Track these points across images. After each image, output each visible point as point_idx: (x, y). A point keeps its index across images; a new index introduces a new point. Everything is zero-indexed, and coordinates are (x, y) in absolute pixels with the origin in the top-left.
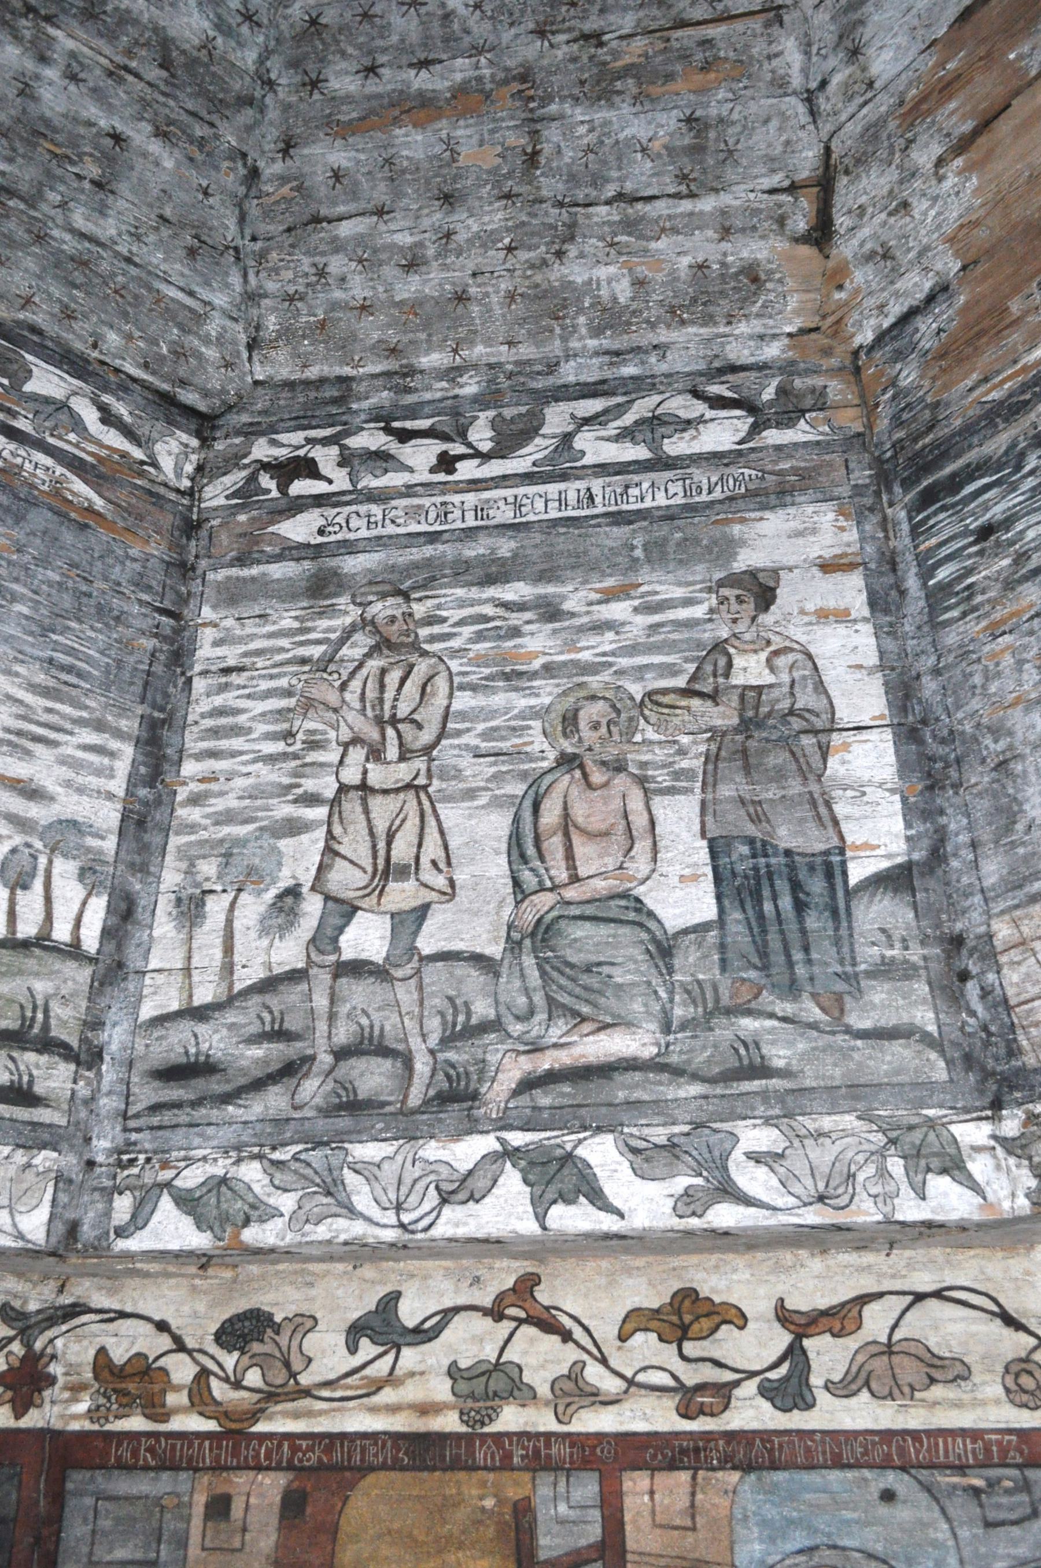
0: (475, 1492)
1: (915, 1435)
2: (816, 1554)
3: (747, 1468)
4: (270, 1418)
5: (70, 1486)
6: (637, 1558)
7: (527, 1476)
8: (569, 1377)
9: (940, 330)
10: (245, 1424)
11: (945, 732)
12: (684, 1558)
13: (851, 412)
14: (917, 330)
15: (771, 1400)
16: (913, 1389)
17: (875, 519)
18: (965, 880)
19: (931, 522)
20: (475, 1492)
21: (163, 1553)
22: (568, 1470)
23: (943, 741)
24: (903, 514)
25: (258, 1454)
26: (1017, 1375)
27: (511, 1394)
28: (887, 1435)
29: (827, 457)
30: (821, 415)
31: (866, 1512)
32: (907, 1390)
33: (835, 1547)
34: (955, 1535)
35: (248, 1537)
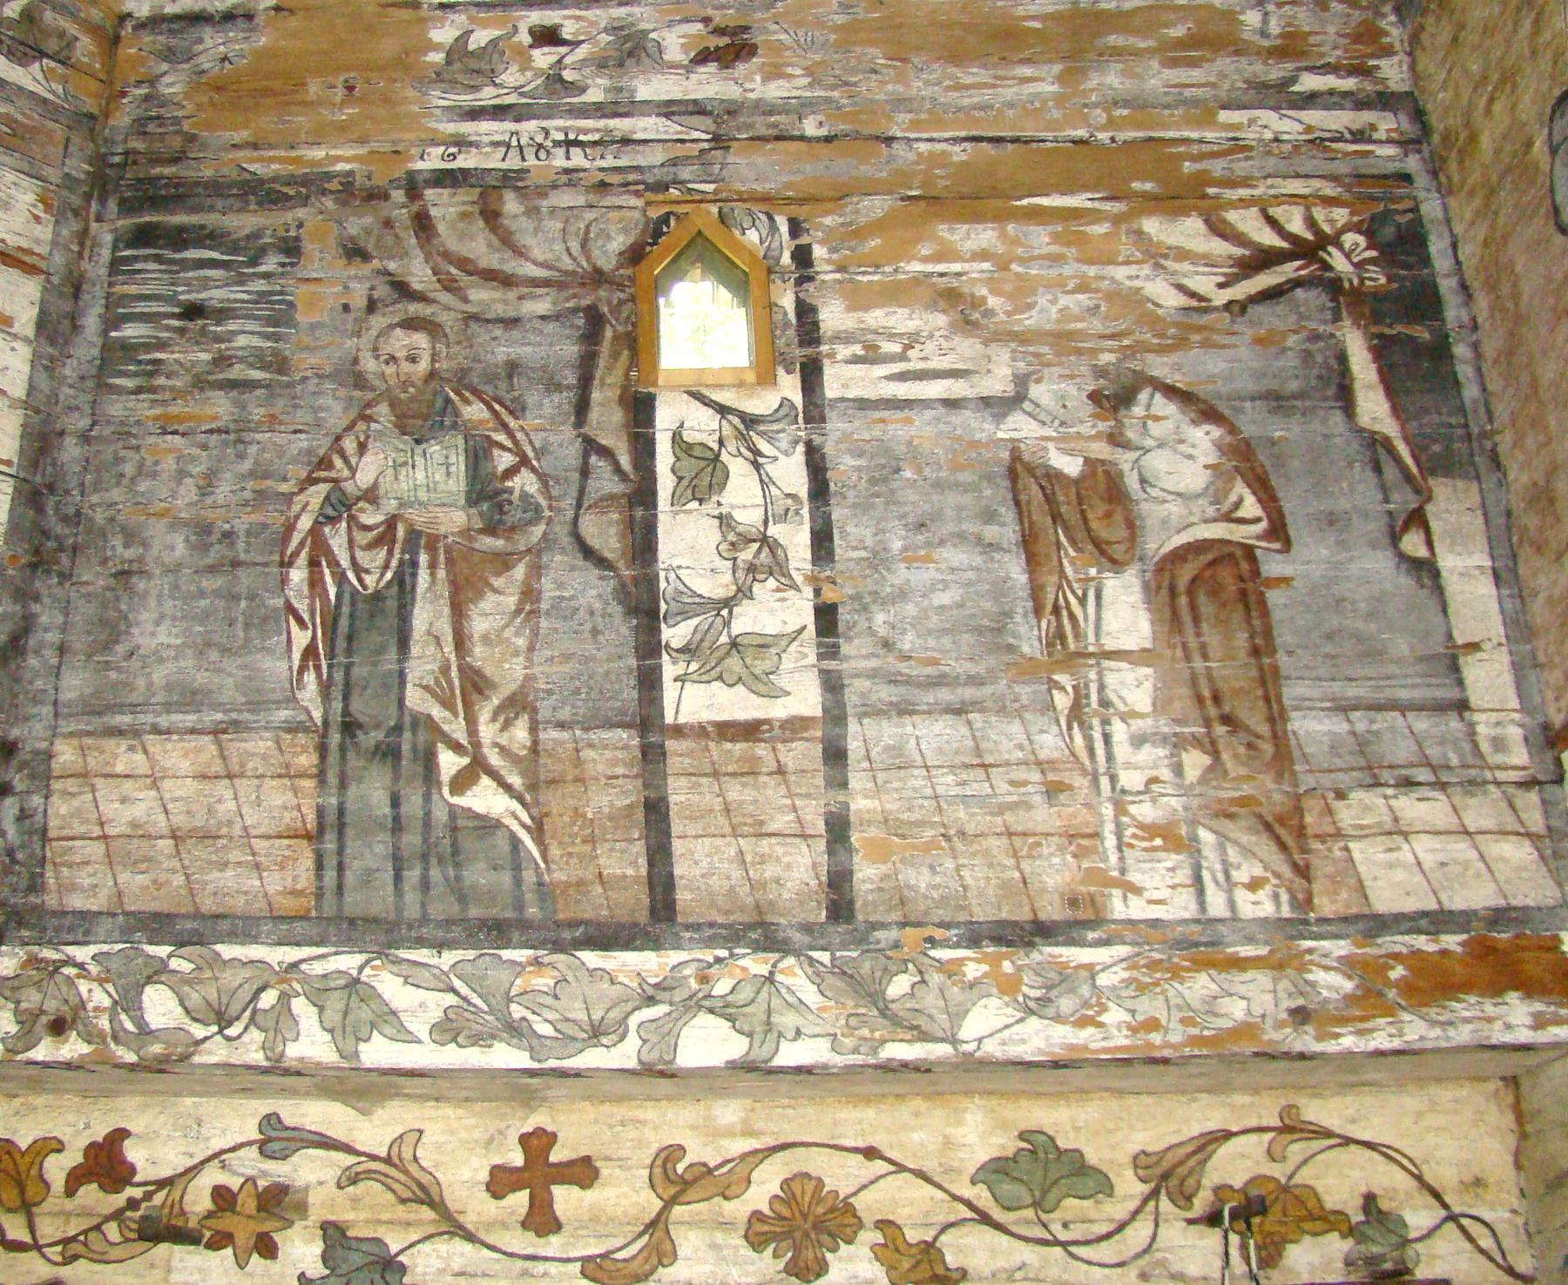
9: (225, 59)
11: (71, 511)
13: (93, 85)
14: (200, 41)
17: (76, 226)
18: (39, 684)
19: (138, 266)
23: (65, 519)
24: (109, 238)
29: (51, 125)
30: (60, 69)
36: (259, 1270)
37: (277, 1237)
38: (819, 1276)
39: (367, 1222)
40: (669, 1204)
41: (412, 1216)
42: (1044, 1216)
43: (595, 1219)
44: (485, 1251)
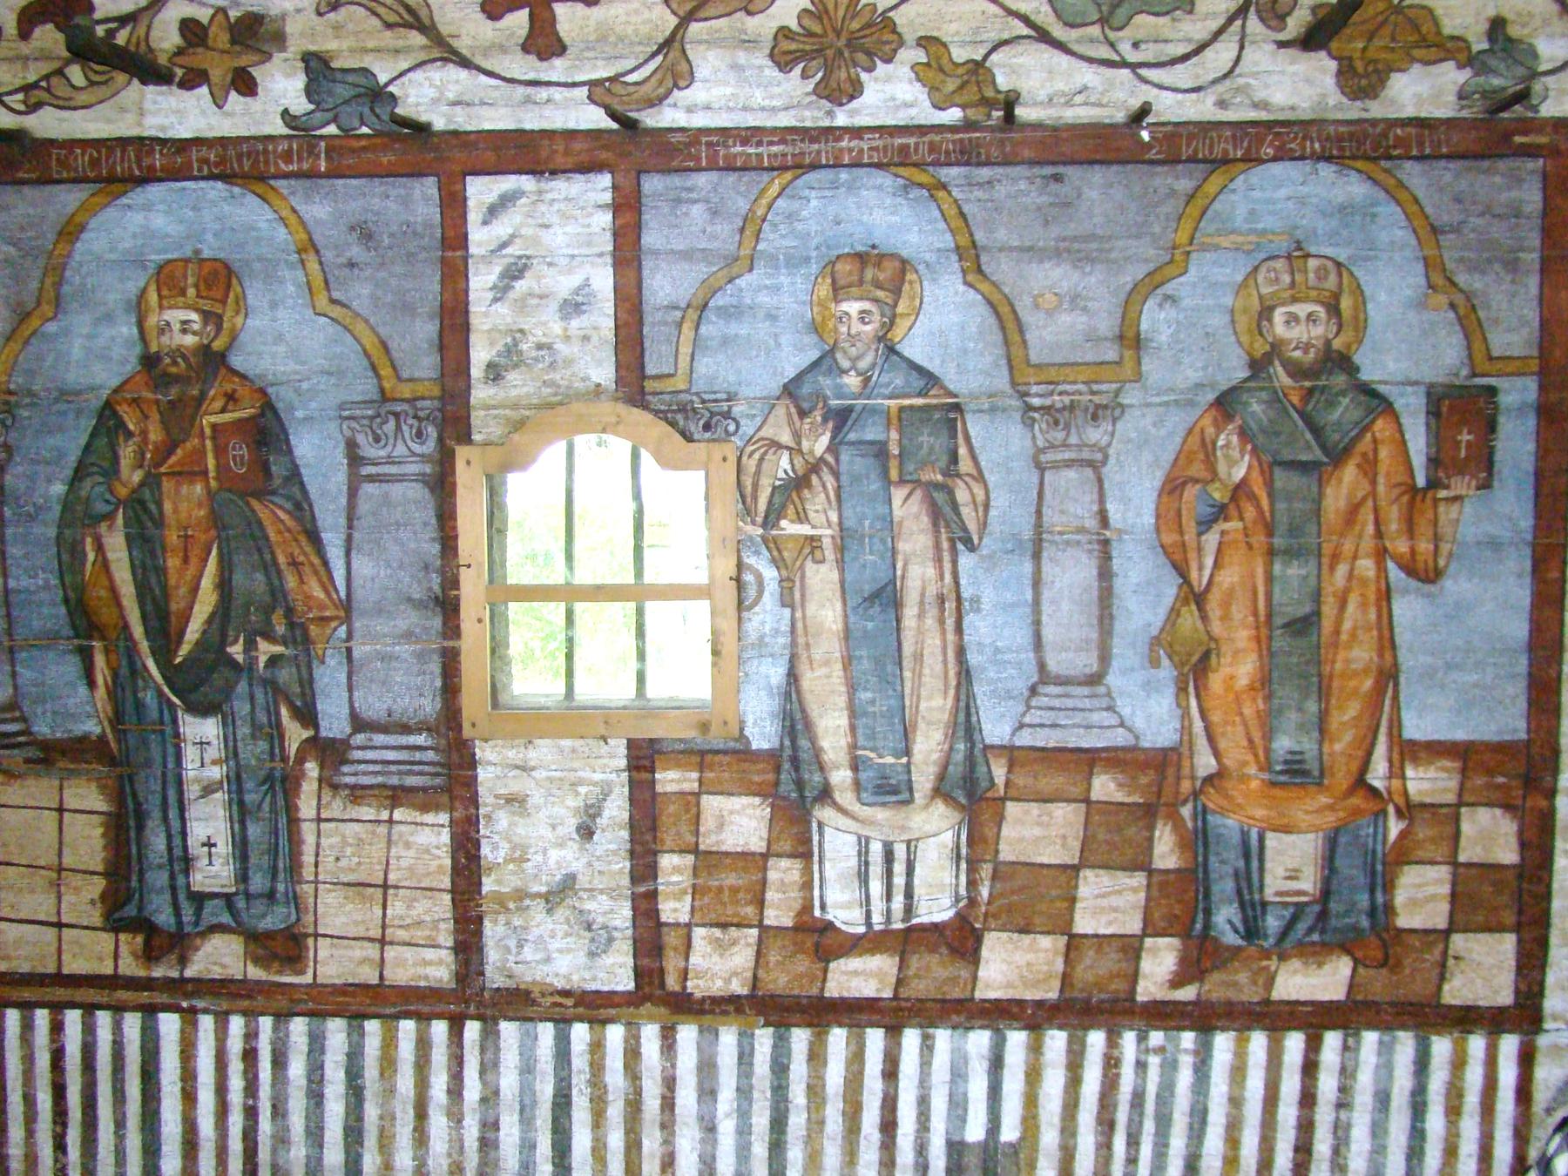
36: (239, 108)
37: (255, 72)
38: (852, 98)
39: (352, 51)
40: (685, 20)
41: (401, 43)
42: (1112, 35)
43: (602, 39)
44: (483, 79)
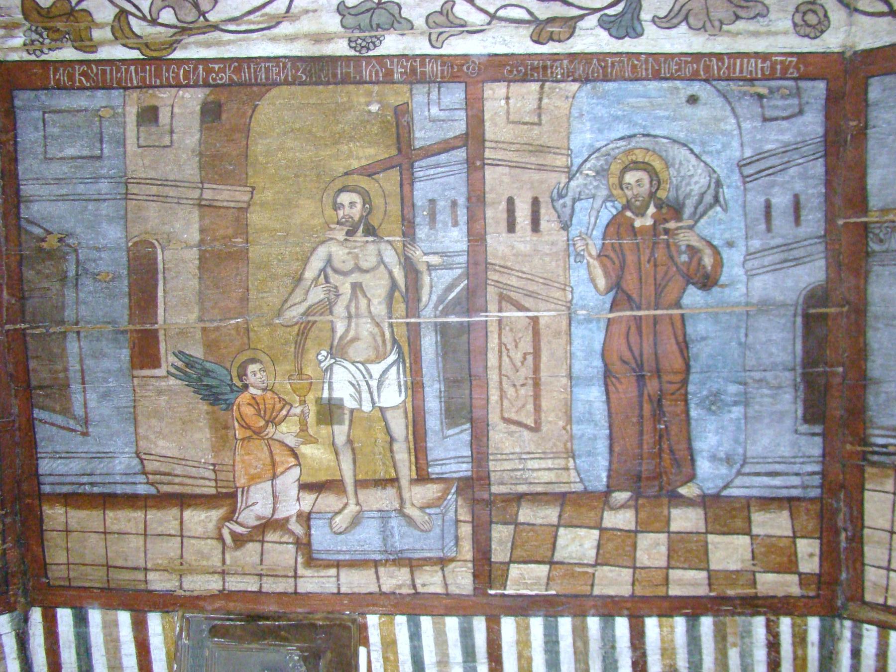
0: (362, 100)
1: (719, 56)
2: (634, 140)
3: (585, 80)
4: (185, 47)
5: (17, 103)
6: (493, 145)
7: (405, 88)
8: (441, 13)
10: (165, 53)
12: (531, 145)
15: (608, 30)
16: (722, 23)
20: (362, 100)
21: (105, 151)
22: (439, 82)
25: (178, 74)
26: (805, 13)
27: (392, 26)
28: (697, 56)
31: (674, 111)
32: (717, 24)
33: (648, 135)
34: (739, 127)
35: (175, 137)
